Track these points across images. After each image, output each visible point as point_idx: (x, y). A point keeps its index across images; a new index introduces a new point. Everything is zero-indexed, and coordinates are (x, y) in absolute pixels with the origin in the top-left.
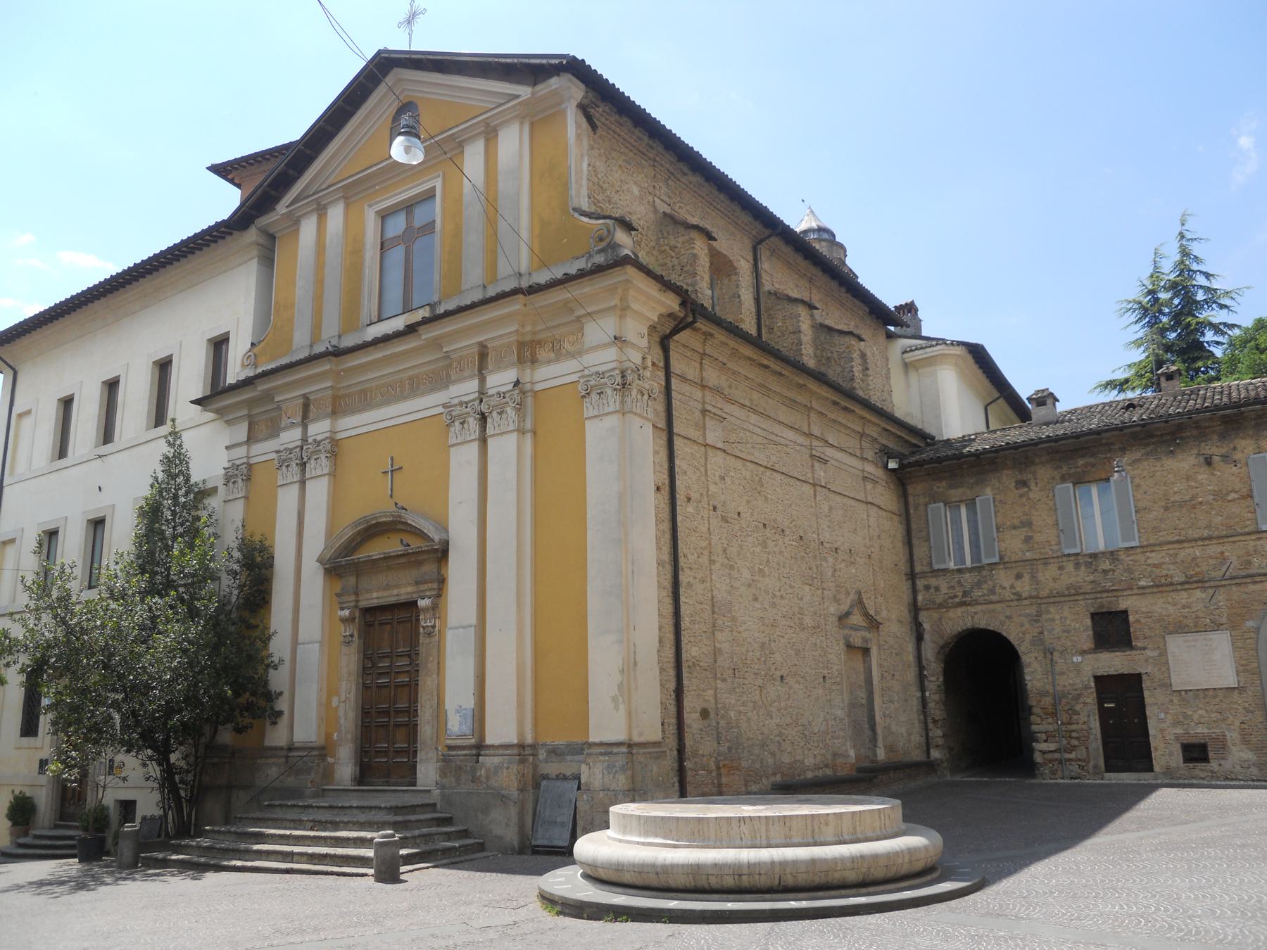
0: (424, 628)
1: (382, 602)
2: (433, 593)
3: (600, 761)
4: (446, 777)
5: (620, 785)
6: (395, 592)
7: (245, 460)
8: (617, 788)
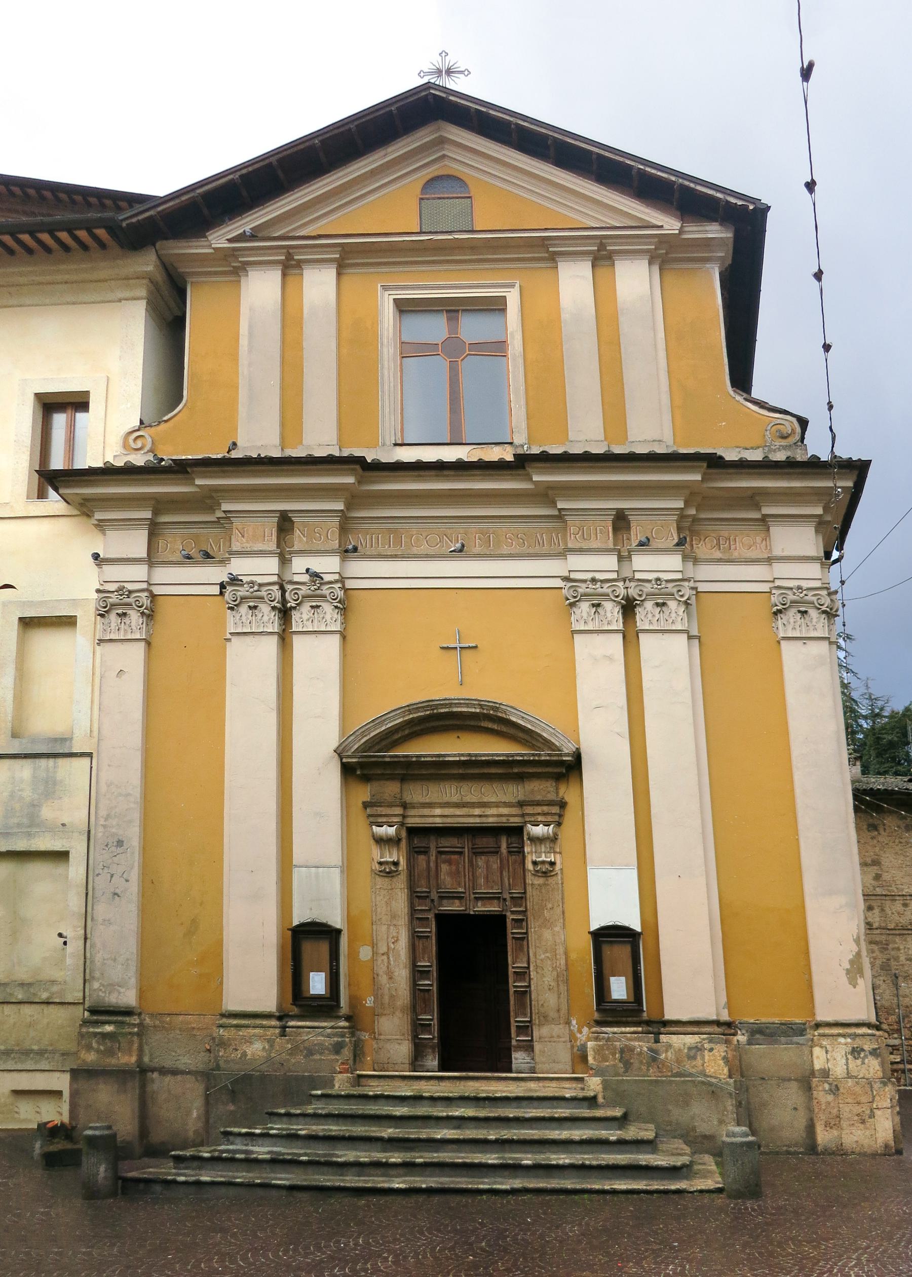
0: (535, 863)
2: (549, 819)
3: (840, 1043)
5: (871, 1070)
7: (144, 586)
8: (867, 1076)
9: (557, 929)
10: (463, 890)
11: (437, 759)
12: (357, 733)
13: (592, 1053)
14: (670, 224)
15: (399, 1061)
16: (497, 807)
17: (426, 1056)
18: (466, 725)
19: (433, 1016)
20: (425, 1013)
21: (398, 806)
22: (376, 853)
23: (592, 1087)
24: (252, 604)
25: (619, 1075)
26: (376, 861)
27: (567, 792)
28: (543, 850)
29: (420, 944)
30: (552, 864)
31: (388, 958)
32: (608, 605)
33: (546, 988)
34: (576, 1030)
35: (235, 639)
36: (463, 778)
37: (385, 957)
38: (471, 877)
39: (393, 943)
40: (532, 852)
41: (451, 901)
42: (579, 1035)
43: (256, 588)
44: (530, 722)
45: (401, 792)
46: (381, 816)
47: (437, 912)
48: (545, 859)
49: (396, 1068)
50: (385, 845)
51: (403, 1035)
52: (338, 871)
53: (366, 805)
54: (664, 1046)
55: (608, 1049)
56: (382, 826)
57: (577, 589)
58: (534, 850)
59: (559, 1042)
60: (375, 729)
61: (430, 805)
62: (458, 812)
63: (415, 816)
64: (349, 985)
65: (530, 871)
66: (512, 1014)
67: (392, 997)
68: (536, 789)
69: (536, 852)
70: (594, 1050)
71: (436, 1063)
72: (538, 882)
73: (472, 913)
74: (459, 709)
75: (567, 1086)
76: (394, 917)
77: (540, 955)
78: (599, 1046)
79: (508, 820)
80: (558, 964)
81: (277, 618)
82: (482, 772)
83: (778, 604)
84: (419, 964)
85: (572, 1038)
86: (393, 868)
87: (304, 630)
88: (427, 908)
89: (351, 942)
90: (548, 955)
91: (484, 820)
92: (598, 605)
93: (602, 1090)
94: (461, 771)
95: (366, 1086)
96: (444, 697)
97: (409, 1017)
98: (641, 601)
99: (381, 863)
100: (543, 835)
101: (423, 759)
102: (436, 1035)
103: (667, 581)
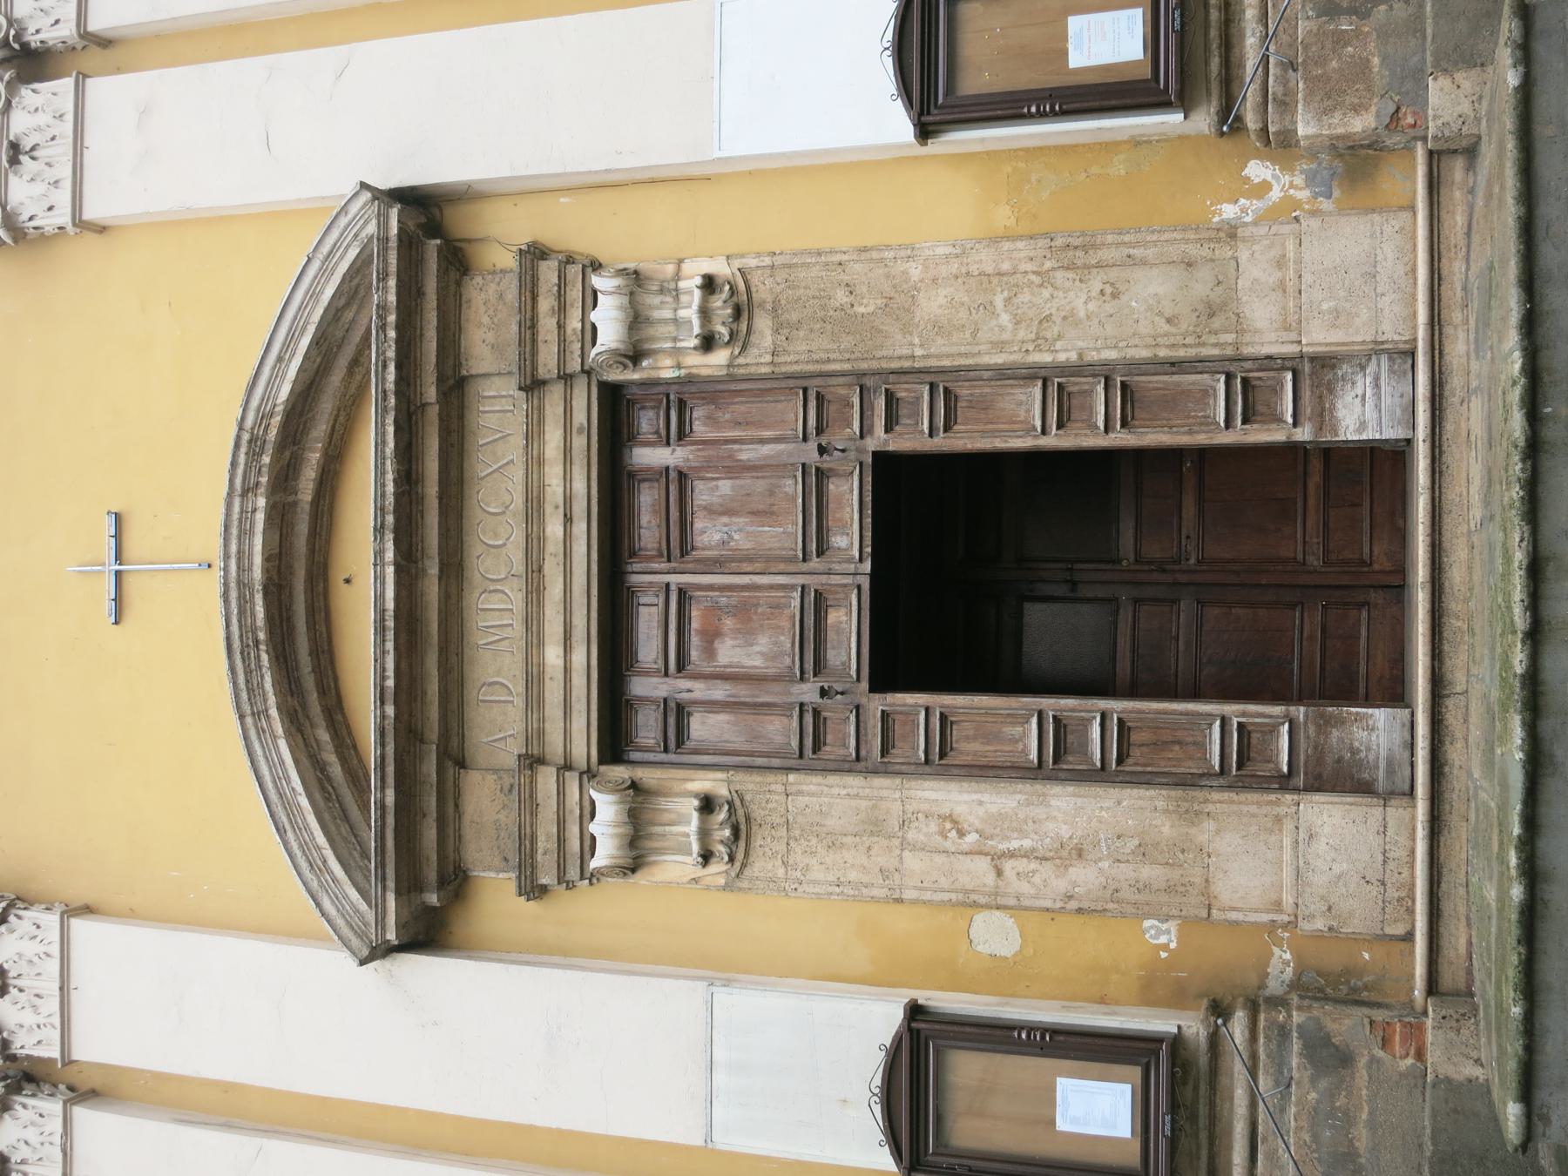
0: (708, 343)
1: (585, 619)
2: (574, 293)
6: (554, 528)
9: (915, 271)
10: (797, 595)
11: (390, 635)
12: (315, 884)
13: (1337, 117)
15: (1375, 841)
16: (541, 462)
17: (1354, 751)
18: (312, 551)
19: (1211, 716)
20: (1202, 747)
21: (533, 782)
23: (1465, 107)
25: (1419, 17)
26: (700, 872)
28: (667, 314)
29: (967, 747)
31: (1012, 855)
33: (1110, 307)
34: (1257, 204)
36: (454, 567)
37: (1009, 866)
38: (758, 566)
39: (961, 834)
40: (677, 352)
41: (831, 635)
42: (1275, 194)
44: (292, 339)
45: (495, 771)
46: (561, 840)
47: (865, 685)
48: (695, 307)
49: (1398, 853)
50: (650, 836)
51: (1278, 819)
52: (722, 996)
53: (533, 890)
55: (1322, 61)
56: (593, 839)
58: (669, 345)
59: (1298, 261)
60: (307, 827)
61: (534, 680)
62: (554, 591)
63: (567, 733)
64: (1102, 1001)
65: (733, 357)
66: (1201, 439)
67: (1144, 852)
68: (490, 337)
69: (675, 339)
70: (1327, 112)
71: (1380, 715)
72: (768, 332)
73: (867, 566)
74: (258, 560)
75: (1460, 219)
76: (874, 826)
77: (1002, 328)
78: (1310, 93)
79: (580, 431)
80: (1030, 267)
82: (436, 502)
84: (1034, 756)
85: (1286, 212)
86: (722, 815)
87: (57, 1020)
88: (853, 718)
89: (956, 983)
90: (999, 301)
91: (579, 508)
93: (1475, 72)
94: (434, 570)
95: (1469, 972)
96: (218, 604)
97: (1215, 796)
99: (706, 857)
100: (621, 308)
101: (390, 683)
102: (1277, 710)
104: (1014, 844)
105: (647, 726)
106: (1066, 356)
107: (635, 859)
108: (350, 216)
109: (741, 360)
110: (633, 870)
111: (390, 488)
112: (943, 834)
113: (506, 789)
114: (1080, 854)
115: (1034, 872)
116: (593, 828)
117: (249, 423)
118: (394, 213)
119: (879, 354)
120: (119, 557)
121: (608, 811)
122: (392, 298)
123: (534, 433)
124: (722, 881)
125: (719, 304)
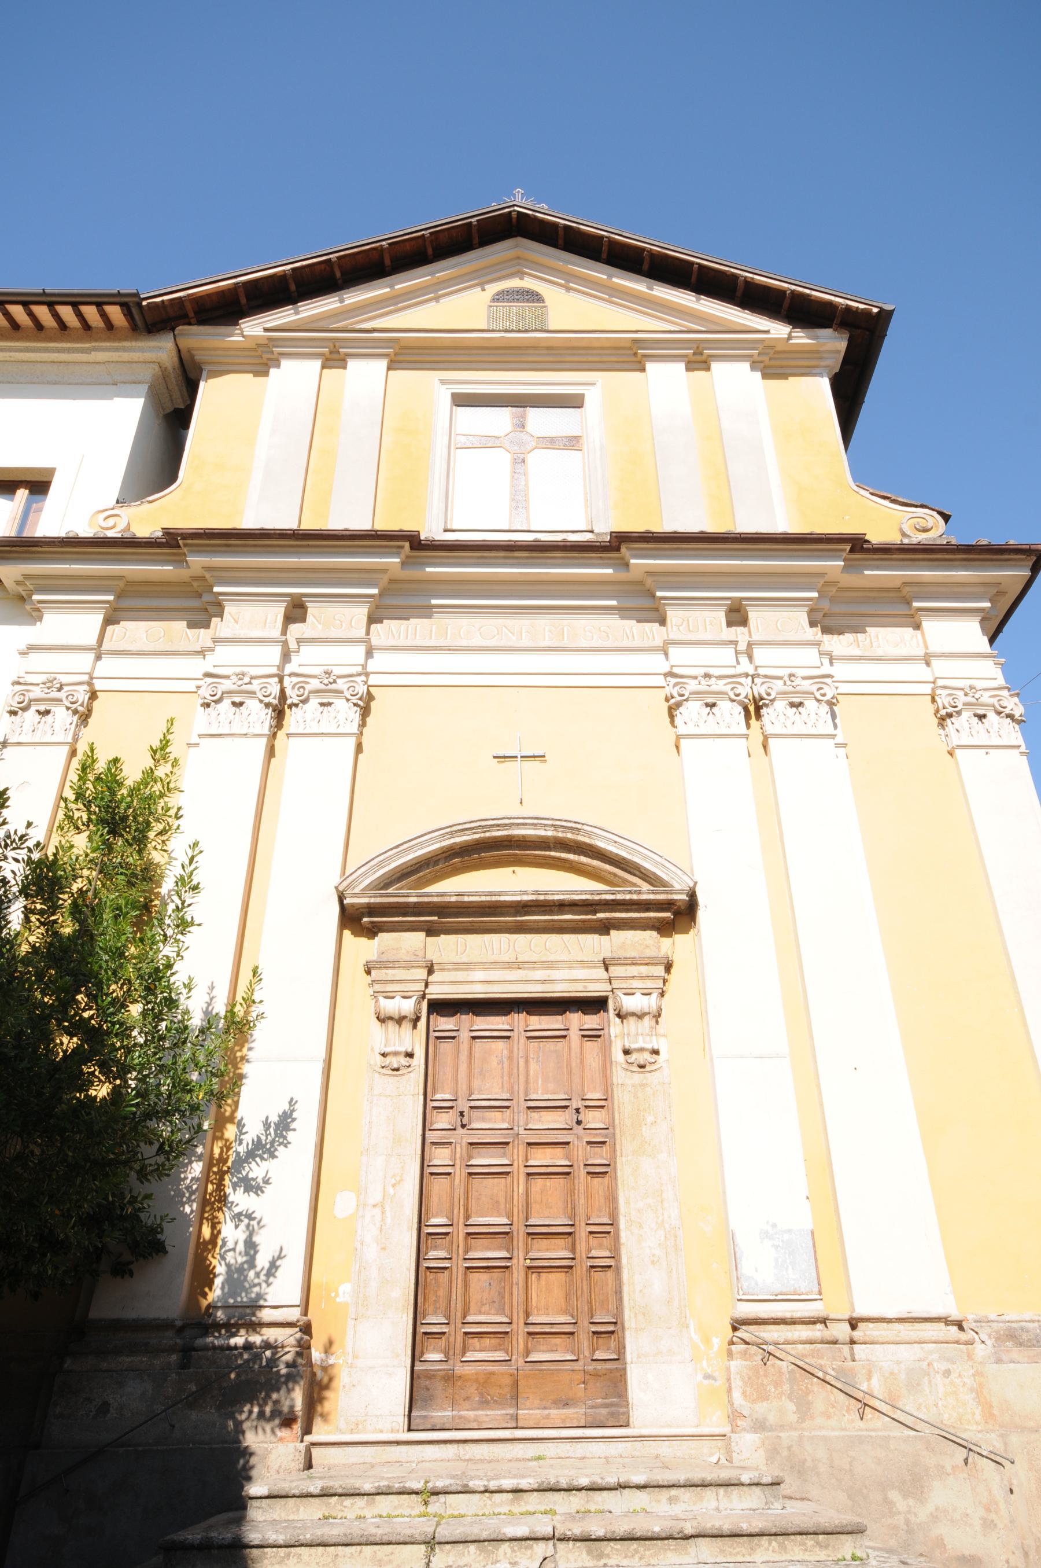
0: (626, 1052)
2: (649, 984)
4: (764, 1397)
6: (540, 974)
13: (740, 1383)
14: (778, 330)
22: (380, 1037)
24: (237, 700)
26: (377, 1051)
27: (677, 946)
30: (656, 1052)
32: (724, 705)
35: (204, 741)
37: (377, 1211)
39: (394, 1186)
43: (247, 680)
54: (863, 1367)
56: (393, 998)
57: (685, 686)
58: (626, 1032)
61: (467, 966)
81: (269, 717)
83: (948, 706)
92: (714, 705)
98: (771, 701)
99: (384, 1055)
103: (804, 678)
104: (388, 1214)
105: (445, 1023)
106: (624, 1236)
107: (383, 1019)
108: (682, 876)
109: (619, 1068)
110: (378, 1018)
111: (556, 897)
112: (394, 1176)
113: (417, 953)
114: (384, 1249)
115: (375, 1224)
116: (398, 998)
117: (585, 827)
118: (684, 897)
119: (623, 1138)
120: (522, 757)
121: (407, 1006)
122: (644, 897)
123: (583, 964)
124: (372, 1063)
125: (645, 1057)
